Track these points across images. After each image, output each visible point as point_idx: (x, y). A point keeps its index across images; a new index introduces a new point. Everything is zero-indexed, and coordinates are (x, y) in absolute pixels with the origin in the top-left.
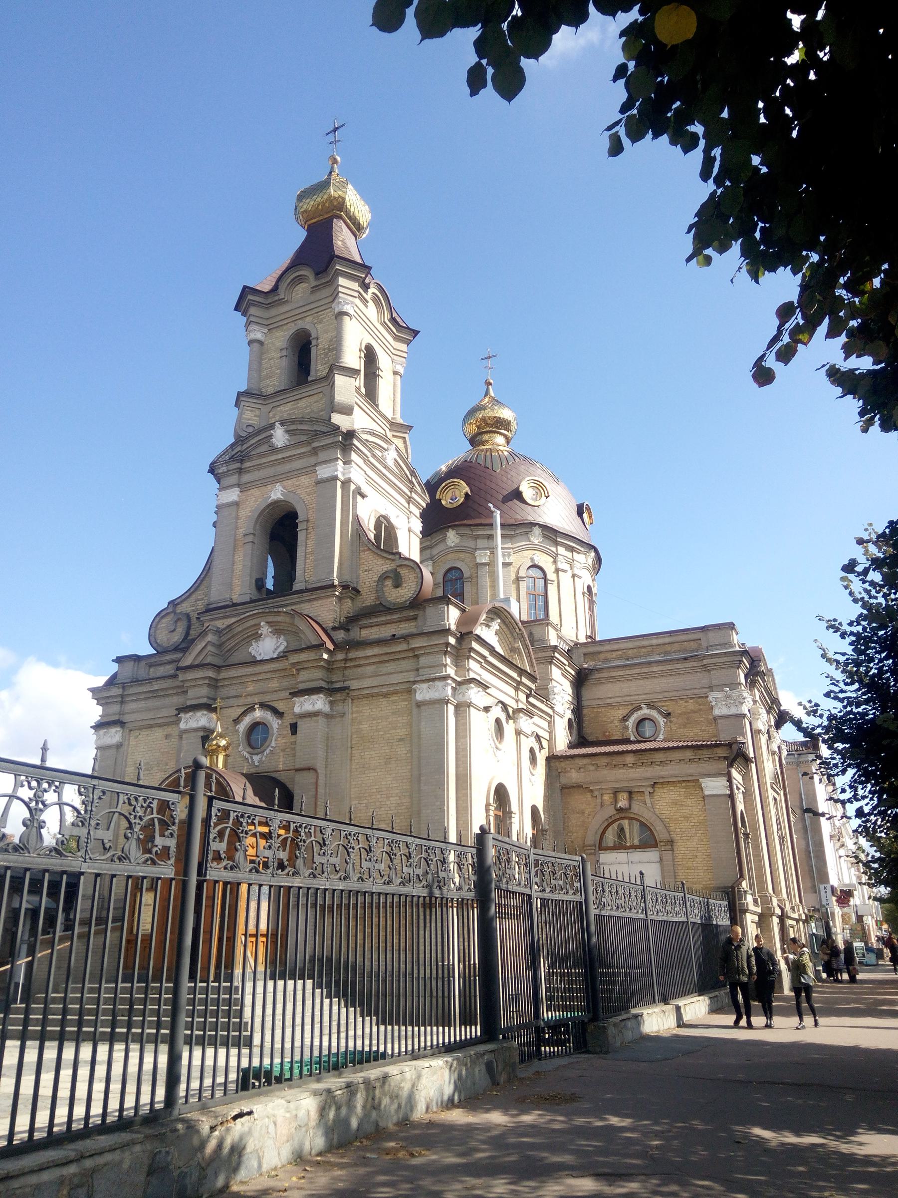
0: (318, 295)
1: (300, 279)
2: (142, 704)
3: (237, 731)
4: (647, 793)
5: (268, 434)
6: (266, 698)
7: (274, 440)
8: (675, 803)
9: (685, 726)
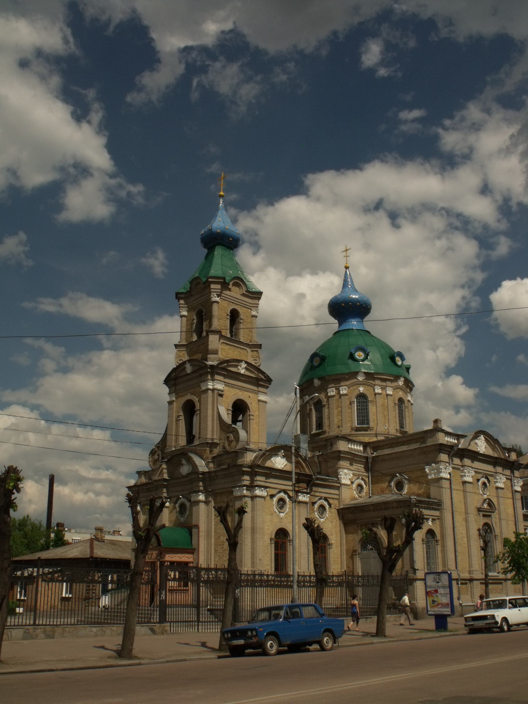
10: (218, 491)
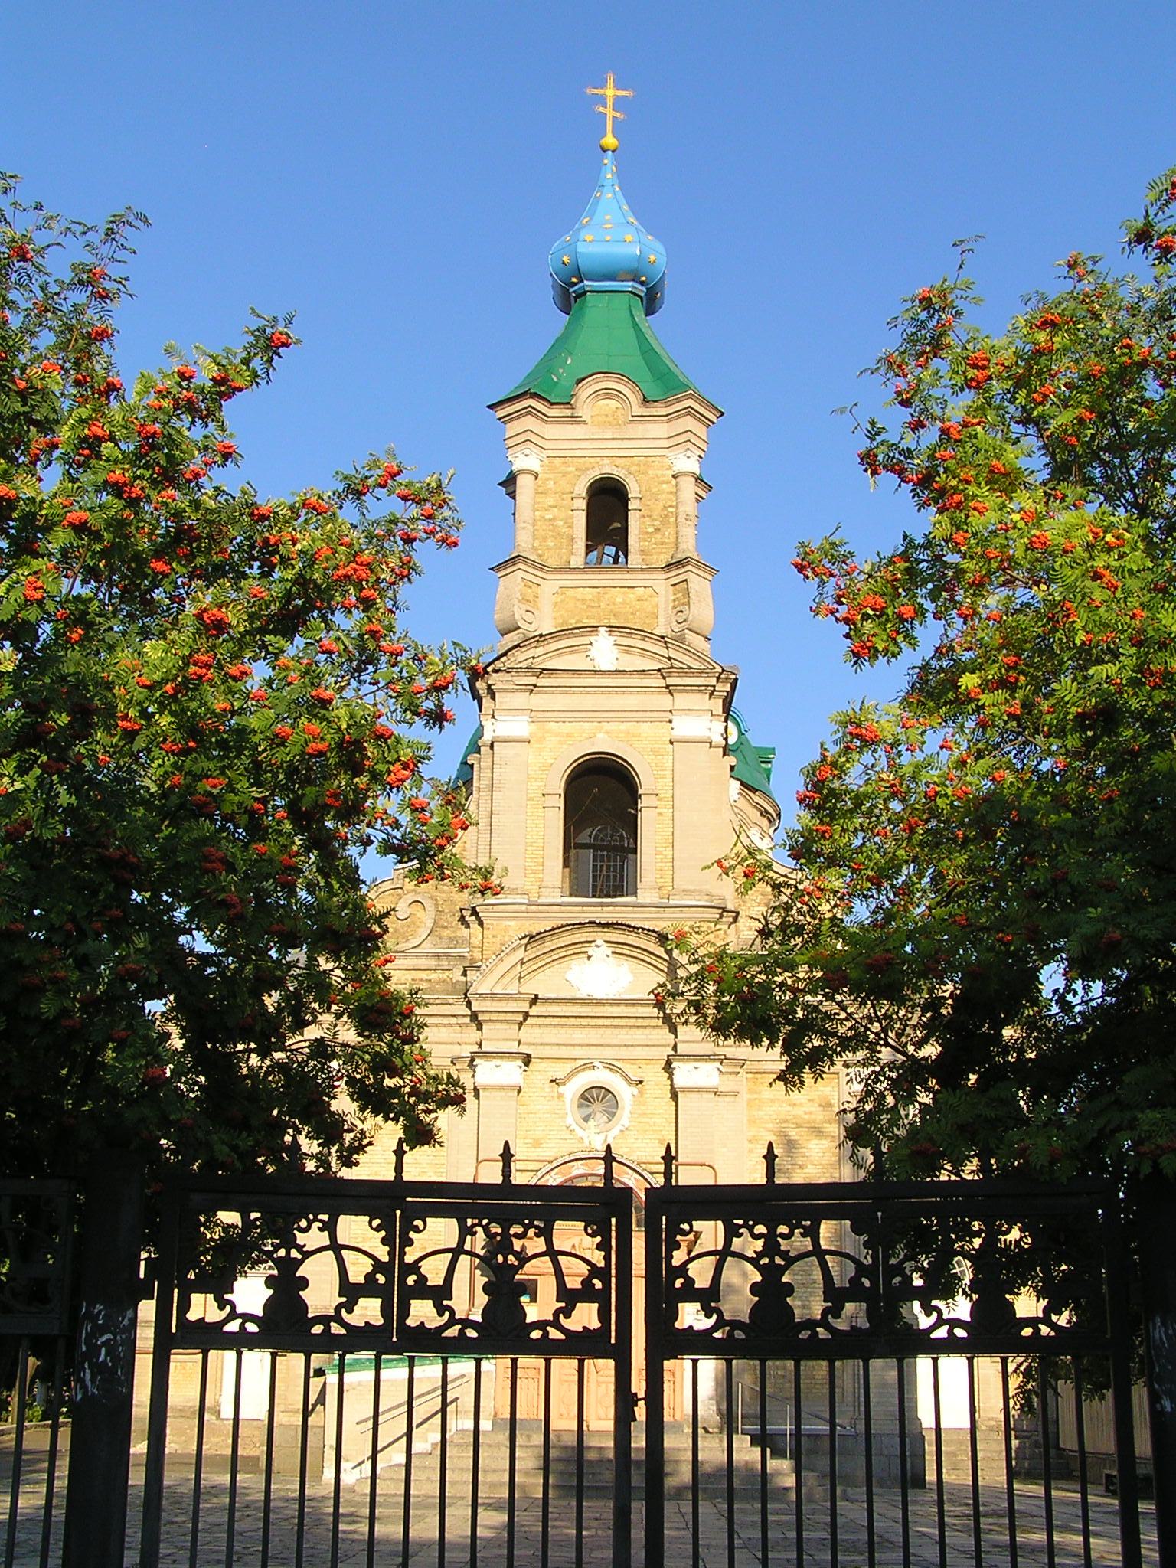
0: (639, 430)
1: (609, 394)
3: (560, 1096)
5: (586, 640)
6: (609, 1054)
7: (593, 652)
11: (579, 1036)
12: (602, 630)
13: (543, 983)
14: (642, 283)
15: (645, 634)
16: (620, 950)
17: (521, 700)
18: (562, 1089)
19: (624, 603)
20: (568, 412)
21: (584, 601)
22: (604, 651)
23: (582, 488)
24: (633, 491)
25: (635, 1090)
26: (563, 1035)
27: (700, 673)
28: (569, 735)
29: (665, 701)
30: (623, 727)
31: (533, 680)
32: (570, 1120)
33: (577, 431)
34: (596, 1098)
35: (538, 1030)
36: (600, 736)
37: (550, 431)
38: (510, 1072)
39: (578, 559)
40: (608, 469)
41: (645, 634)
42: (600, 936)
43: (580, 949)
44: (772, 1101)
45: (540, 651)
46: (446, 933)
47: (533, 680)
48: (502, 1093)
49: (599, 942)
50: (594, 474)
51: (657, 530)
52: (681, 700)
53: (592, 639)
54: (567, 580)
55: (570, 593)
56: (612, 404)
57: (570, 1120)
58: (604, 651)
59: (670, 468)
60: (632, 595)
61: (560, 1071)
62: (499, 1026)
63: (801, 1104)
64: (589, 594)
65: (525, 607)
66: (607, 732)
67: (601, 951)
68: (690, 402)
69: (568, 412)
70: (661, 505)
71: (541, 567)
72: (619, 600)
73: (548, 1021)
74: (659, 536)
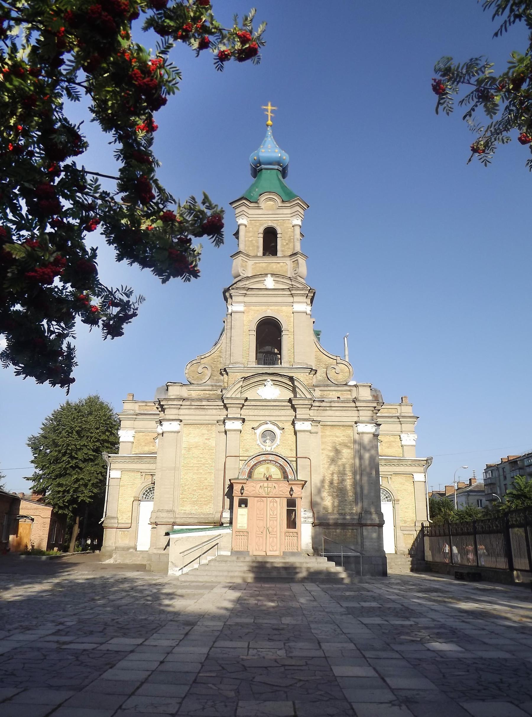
0: (281, 211)
1: (271, 199)
2: (192, 412)
3: (255, 433)
4: (389, 478)
5: (263, 279)
6: (272, 419)
7: (266, 283)
8: (401, 483)
9: (388, 448)
10: (329, 423)
11: (262, 413)
12: (269, 275)
13: (249, 394)
14: (281, 166)
15: (284, 277)
16: (276, 383)
17: (241, 299)
18: (256, 431)
19: (276, 268)
20: (257, 205)
21: (262, 267)
22: (269, 282)
23: (261, 230)
24: (279, 231)
25: (281, 431)
26: (256, 412)
27: (302, 289)
28: (258, 311)
29: (291, 299)
30: (276, 308)
31: (245, 292)
32: (258, 442)
33: (260, 212)
34: (269, 435)
35: (247, 411)
36: (268, 311)
37: (251, 212)
38: (238, 425)
39: (260, 253)
40: (270, 224)
41: (284, 277)
42: (269, 378)
43: (262, 383)
44: (330, 435)
45: (248, 282)
46: (215, 378)
47: (245, 292)
48: (235, 432)
49: (269, 380)
50: (266, 226)
51: (287, 244)
52: (296, 299)
53: (266, 278)
54: (257, 260)
55: (258, 265)
56: (271, 203)
57: (258, 442)
58: (269, 282)
59: (291, 224)
60: (279, 265)
61: (255, 425)
62: (233, 409)
63: (340, 437)
64: (264, 265)
65: (243, 269)
66: (271, 310)
67: (269, 383)
68: (298, 201)
69: (257, 205)
70: (288, 236)
71: (248, 255)
72: (274, 267)
73: (251, 407)
74: (288, 246)
